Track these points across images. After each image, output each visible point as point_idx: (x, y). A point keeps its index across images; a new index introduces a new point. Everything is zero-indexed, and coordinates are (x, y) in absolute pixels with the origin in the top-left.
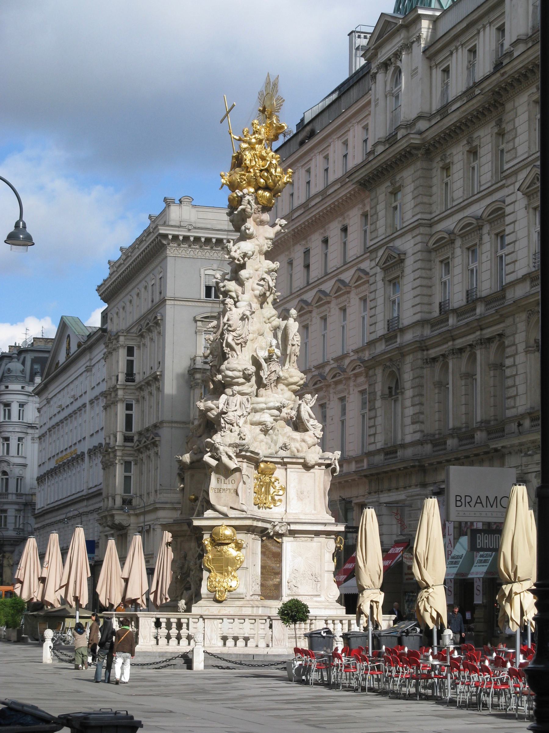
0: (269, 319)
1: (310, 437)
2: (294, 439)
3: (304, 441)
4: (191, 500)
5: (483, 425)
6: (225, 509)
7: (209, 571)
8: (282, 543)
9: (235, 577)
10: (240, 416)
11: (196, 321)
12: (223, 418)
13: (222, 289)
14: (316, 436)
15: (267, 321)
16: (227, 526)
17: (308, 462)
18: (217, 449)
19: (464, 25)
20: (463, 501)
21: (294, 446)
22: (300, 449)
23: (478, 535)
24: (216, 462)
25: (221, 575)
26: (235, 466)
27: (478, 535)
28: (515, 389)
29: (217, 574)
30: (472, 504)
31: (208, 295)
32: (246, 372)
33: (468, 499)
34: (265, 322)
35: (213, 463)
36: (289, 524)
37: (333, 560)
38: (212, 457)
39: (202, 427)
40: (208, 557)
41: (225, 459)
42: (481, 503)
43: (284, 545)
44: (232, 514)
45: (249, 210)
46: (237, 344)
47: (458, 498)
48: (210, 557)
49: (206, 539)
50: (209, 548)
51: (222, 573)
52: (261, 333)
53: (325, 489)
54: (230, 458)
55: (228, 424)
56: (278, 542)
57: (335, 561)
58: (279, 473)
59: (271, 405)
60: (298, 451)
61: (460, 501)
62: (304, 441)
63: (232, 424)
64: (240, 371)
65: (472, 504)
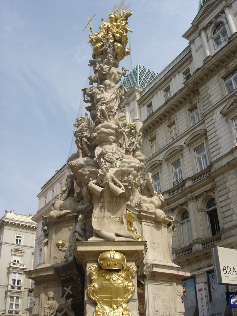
0: (121, 118)
1: (157, 200)
2: (145, 201)
3: (152, 202)
4: (58, 245)
5: (199, 240)
6: (112, 235)
7: (95, 304)
8: (144, 284)
9: (126, 310)
10: (117, 159)
11: (12, 251)
12: (103, 158)
13: (90, 93)
14: (161, 200)
15: (120, 119)
16: (116, 251)
17: (159, 216)
18: (103, 176)
19: (163, 79)
20: (227, 269)
21: (145, 206)
22: (150, 207)
23: (231, 295)
24: (103, 189)
25: (110, 309)
26: (123, 191)
27: (231, 295)
28: (231, 211)
29: (105, 307)
30: (232, 272)
31: (17, 243)
32: (119, 130)
33: (229, 270)
34: (119, 119)
35: (100, 189)
36: (153, 265)
37: (182, 302)
38: (97, 184)
39: (66, 192)
40: (94, 287)
41: (112, 185)
42: (235, 272)
43: (146, 286)
44: (117, 239)
45: (109, 50)
46: (109, 115)
47: (225, 268)
48: (96, 286)
49: (91, 267)
50: (95, 277)
51: (111, 306)
52: (118, 123)
53: (169, 243)
54: (115, 183)
55: (108, 162)
56: (141, 284)
57: (184, 304)
58: (135, 224)
59: (132, 164)
60: (148, 209)
61: (225, 270)
62: (152, 202)
63: (111, 163)
64: (113, 129)
65: (232, 272)
